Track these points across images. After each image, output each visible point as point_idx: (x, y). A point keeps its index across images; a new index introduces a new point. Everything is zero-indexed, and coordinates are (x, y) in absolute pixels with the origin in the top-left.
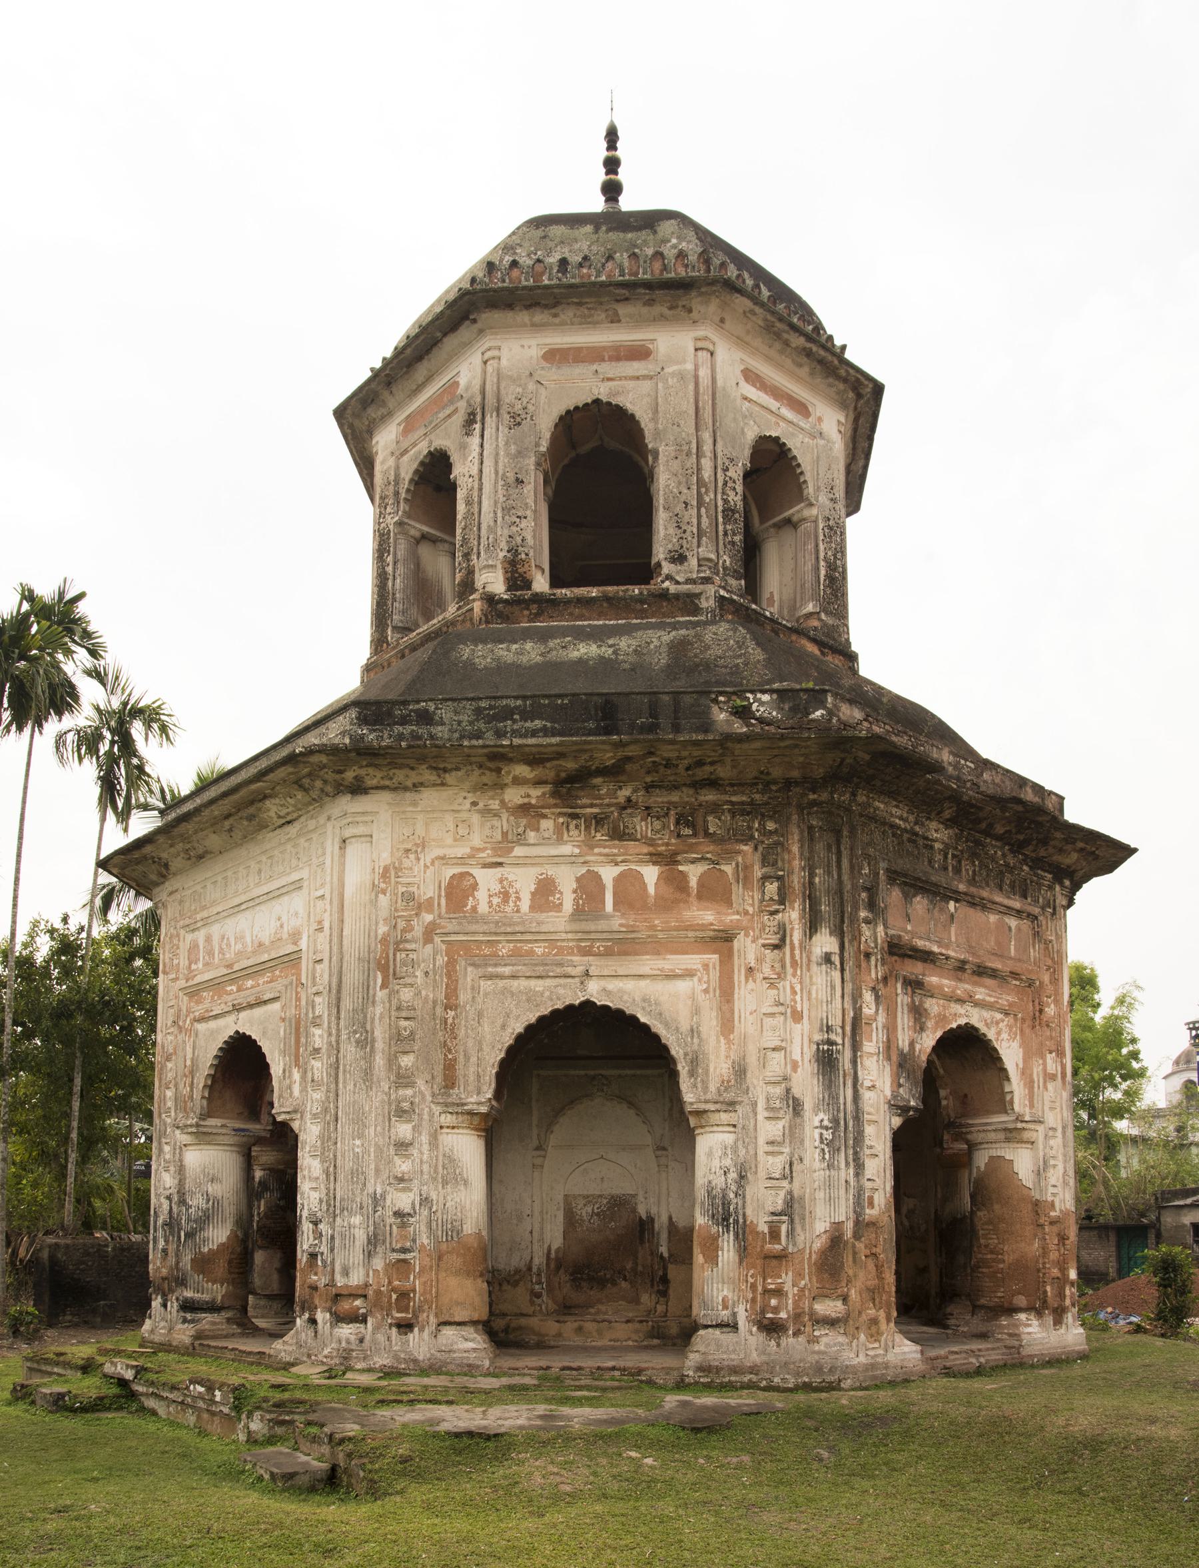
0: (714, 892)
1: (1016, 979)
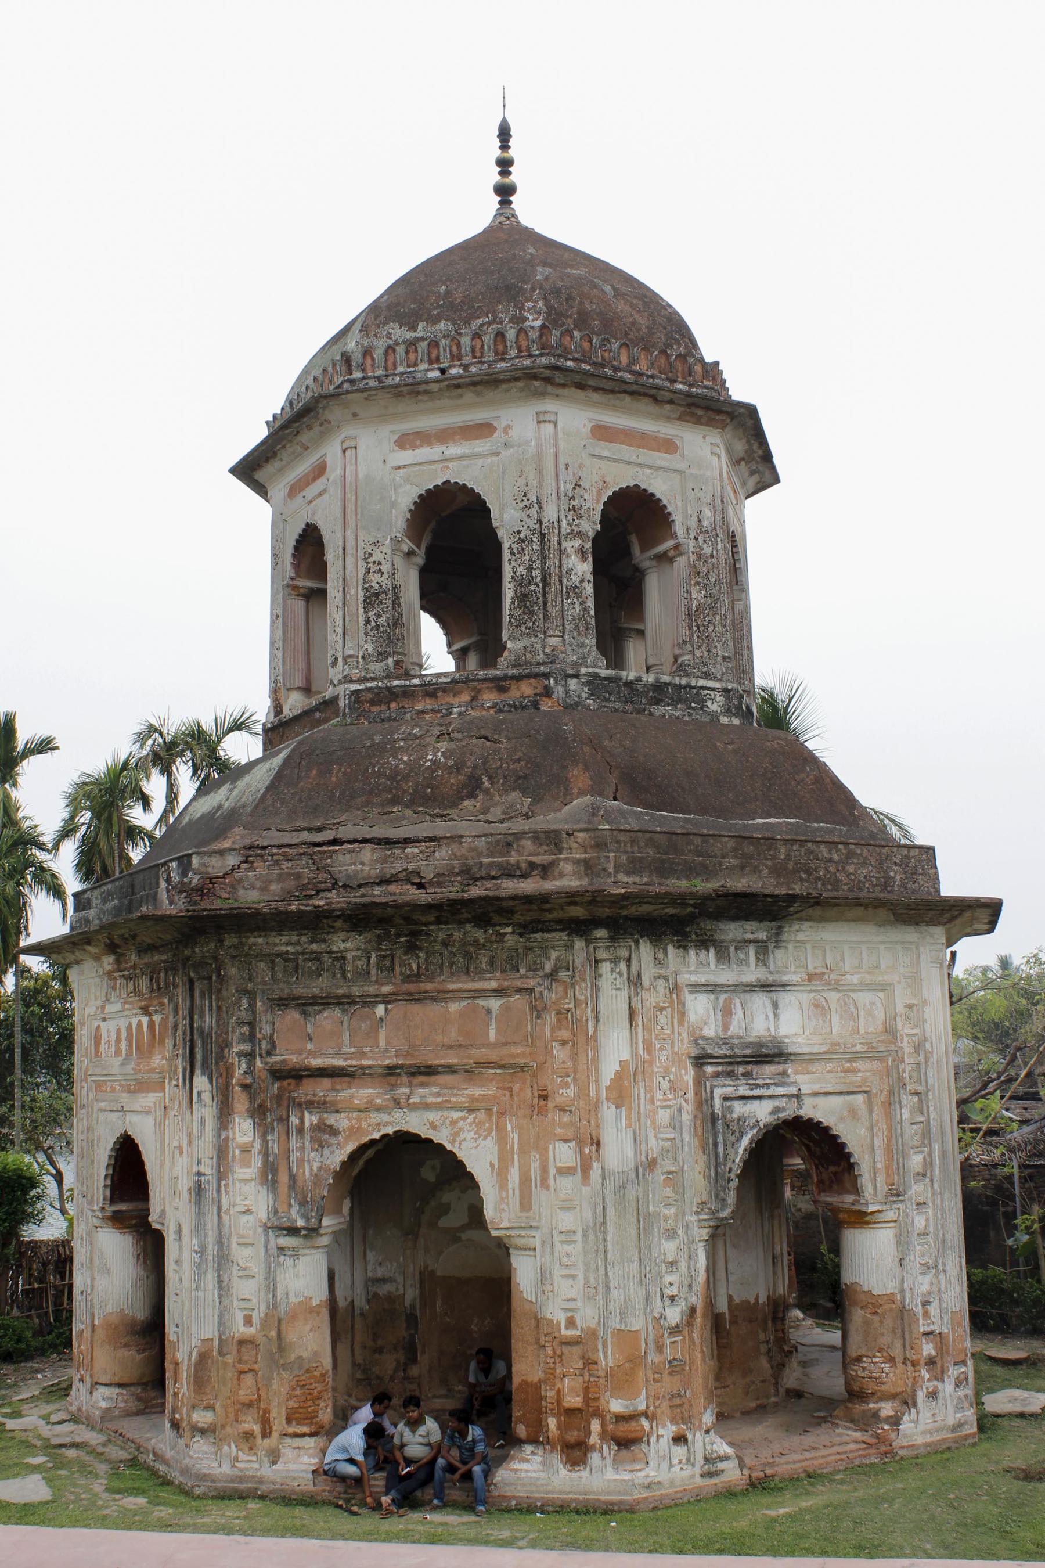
1: (493, 1068)
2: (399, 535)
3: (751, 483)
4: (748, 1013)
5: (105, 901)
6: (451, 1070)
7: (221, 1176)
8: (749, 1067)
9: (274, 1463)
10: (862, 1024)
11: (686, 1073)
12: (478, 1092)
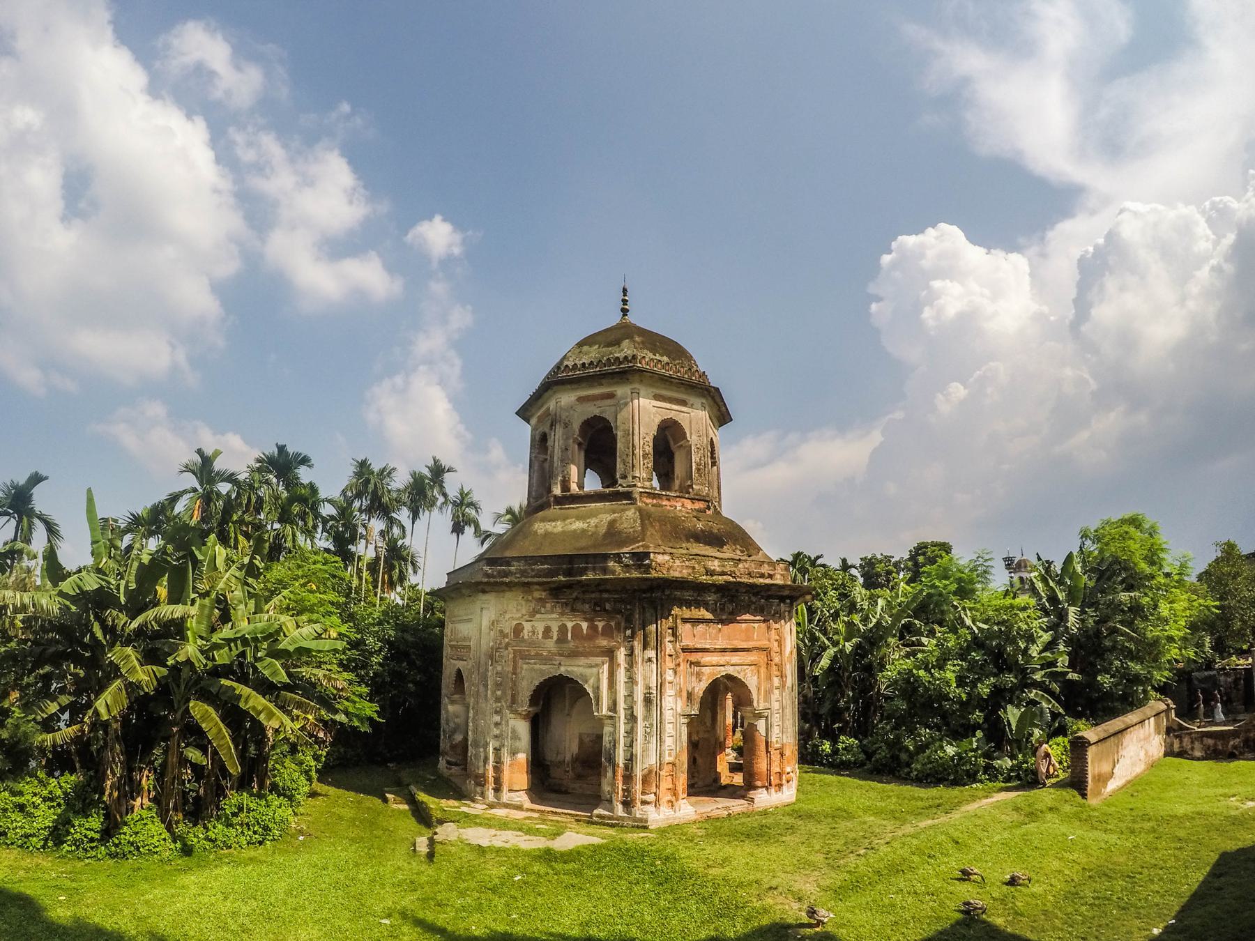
0: (607, 633)
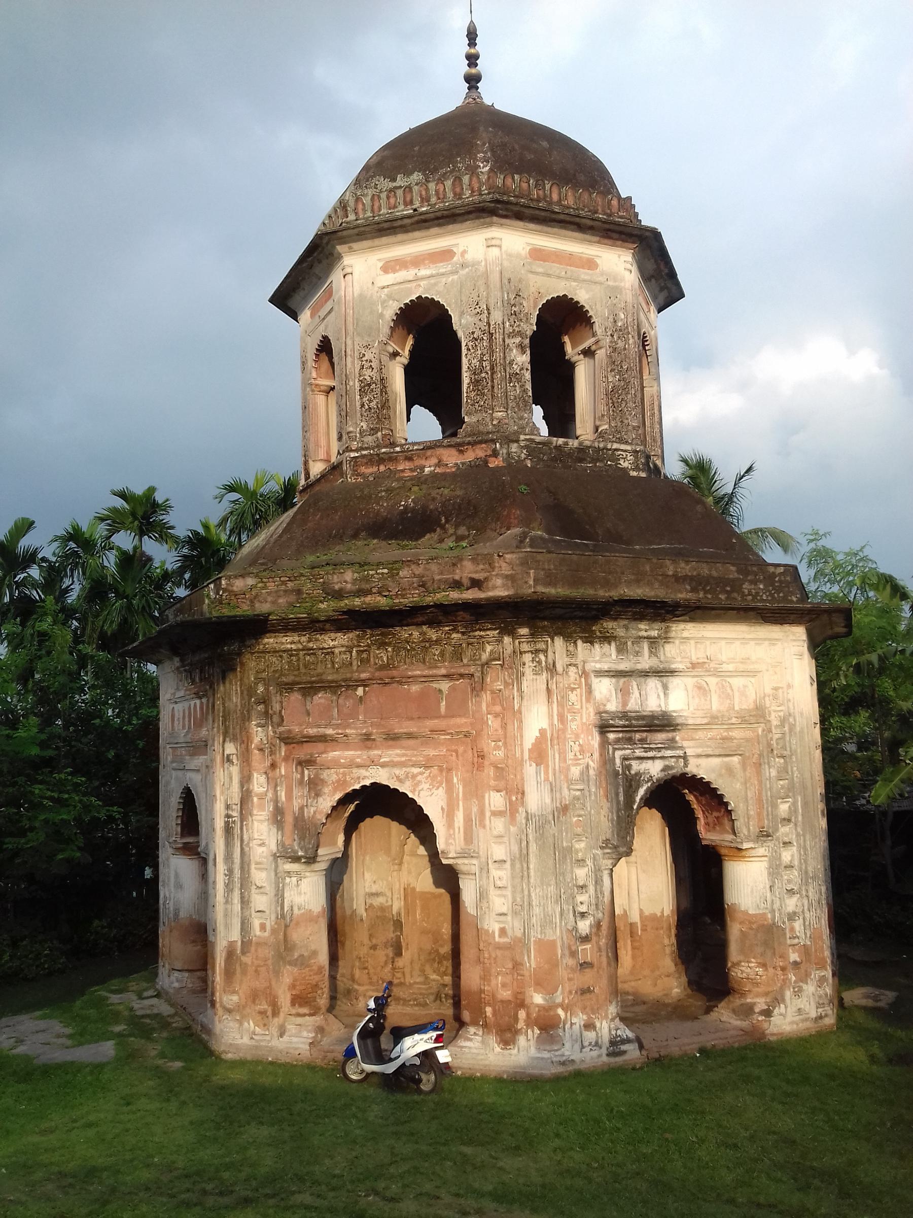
2: (384, 339)
3: (662, 298)
4: (643, 693)
5: (176, 616)
6: (410, 736)
7: (243, 818)
8: (644, 735)
9: (281, 1035)
10: (737, 700)
11: (592, 739)
12: (432, 752)
